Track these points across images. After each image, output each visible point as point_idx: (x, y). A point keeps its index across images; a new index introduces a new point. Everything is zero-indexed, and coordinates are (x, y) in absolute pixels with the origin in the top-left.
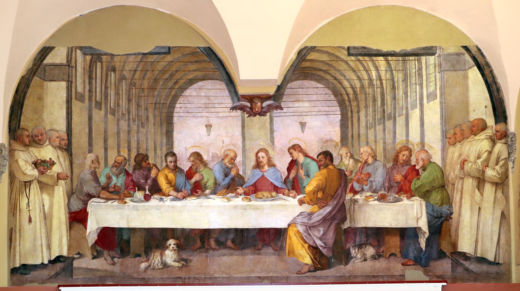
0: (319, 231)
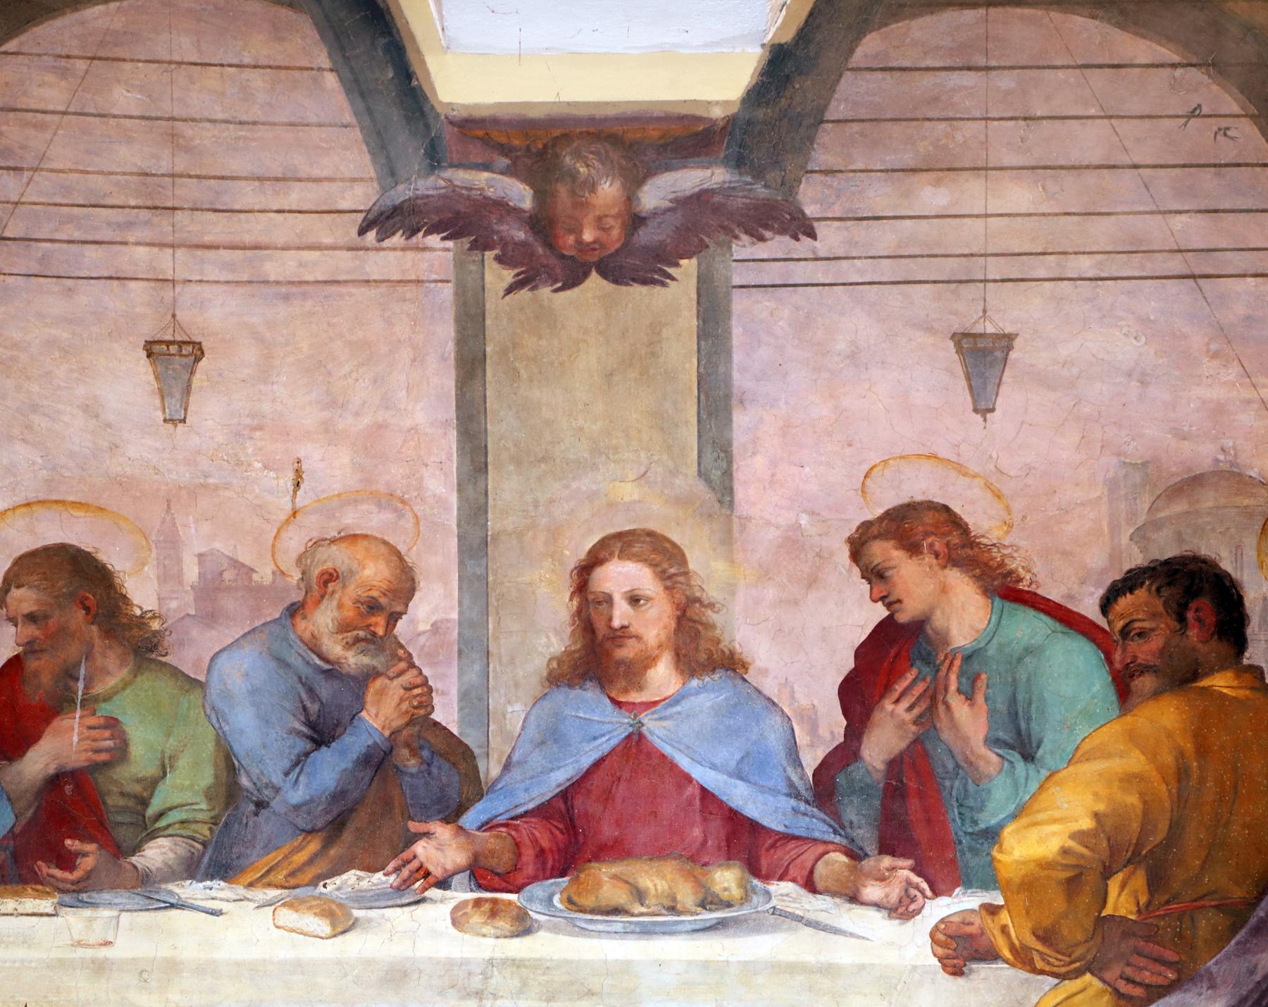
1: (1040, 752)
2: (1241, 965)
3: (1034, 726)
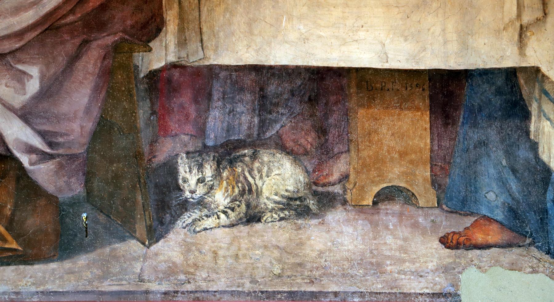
0: (22, 77)
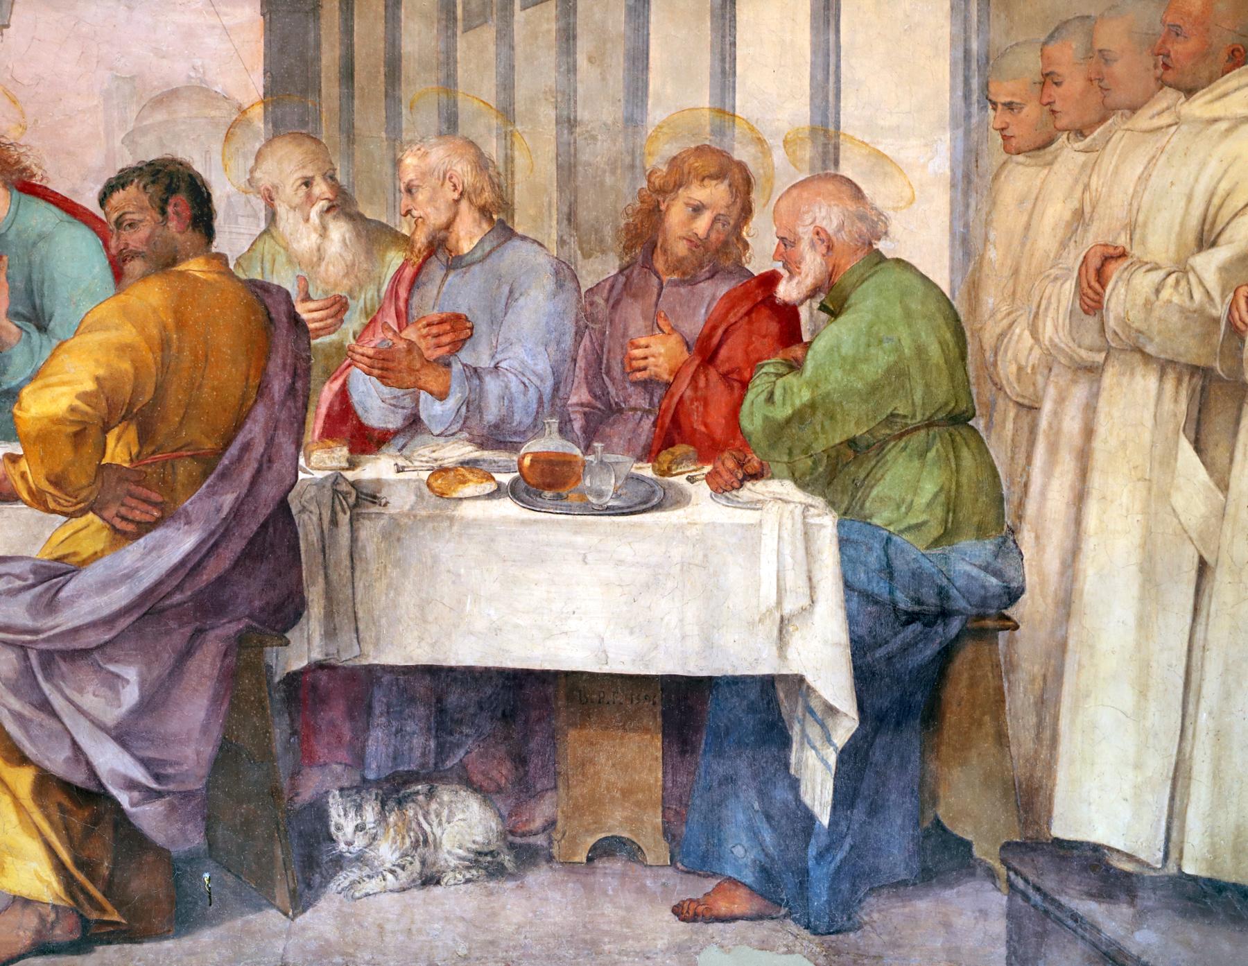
0: (114, 682)
1: (52, 324)
2: (209, 505)
3: (47, 302)
